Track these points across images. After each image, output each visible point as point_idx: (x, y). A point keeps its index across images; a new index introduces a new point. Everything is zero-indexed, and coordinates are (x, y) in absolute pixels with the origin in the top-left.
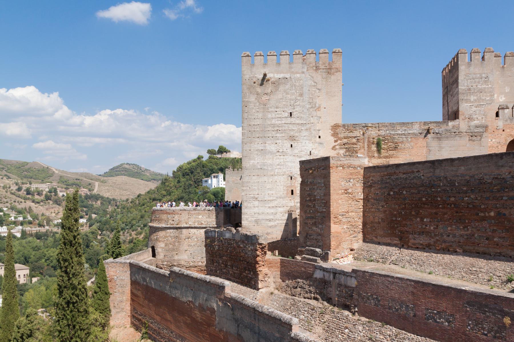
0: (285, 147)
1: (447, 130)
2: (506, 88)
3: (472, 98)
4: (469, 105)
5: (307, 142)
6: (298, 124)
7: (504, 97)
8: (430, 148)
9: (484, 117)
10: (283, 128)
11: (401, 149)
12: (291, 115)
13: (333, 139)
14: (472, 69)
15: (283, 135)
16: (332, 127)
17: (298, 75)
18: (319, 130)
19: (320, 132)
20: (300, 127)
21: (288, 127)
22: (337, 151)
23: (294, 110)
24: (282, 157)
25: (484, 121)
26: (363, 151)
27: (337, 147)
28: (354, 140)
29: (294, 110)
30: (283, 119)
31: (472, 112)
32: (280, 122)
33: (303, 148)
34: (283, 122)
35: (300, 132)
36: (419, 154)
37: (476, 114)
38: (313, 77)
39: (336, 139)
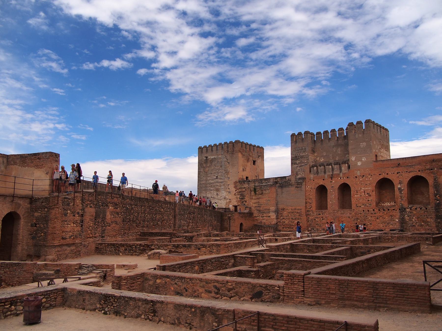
1: (285, 182)
2: (324, 153)
3: (298, 162)
6: (220, 182)
8: (277, 193)
11: (264, 194)
13: (234, 189)
14: (297, 144)
15: (214, 188)
17: (220, 156)
22: (236, 196)
26: (248, 195)
27: (236, 194)
34: (214, 181)
35: (221, 186)
36: (272, 197)
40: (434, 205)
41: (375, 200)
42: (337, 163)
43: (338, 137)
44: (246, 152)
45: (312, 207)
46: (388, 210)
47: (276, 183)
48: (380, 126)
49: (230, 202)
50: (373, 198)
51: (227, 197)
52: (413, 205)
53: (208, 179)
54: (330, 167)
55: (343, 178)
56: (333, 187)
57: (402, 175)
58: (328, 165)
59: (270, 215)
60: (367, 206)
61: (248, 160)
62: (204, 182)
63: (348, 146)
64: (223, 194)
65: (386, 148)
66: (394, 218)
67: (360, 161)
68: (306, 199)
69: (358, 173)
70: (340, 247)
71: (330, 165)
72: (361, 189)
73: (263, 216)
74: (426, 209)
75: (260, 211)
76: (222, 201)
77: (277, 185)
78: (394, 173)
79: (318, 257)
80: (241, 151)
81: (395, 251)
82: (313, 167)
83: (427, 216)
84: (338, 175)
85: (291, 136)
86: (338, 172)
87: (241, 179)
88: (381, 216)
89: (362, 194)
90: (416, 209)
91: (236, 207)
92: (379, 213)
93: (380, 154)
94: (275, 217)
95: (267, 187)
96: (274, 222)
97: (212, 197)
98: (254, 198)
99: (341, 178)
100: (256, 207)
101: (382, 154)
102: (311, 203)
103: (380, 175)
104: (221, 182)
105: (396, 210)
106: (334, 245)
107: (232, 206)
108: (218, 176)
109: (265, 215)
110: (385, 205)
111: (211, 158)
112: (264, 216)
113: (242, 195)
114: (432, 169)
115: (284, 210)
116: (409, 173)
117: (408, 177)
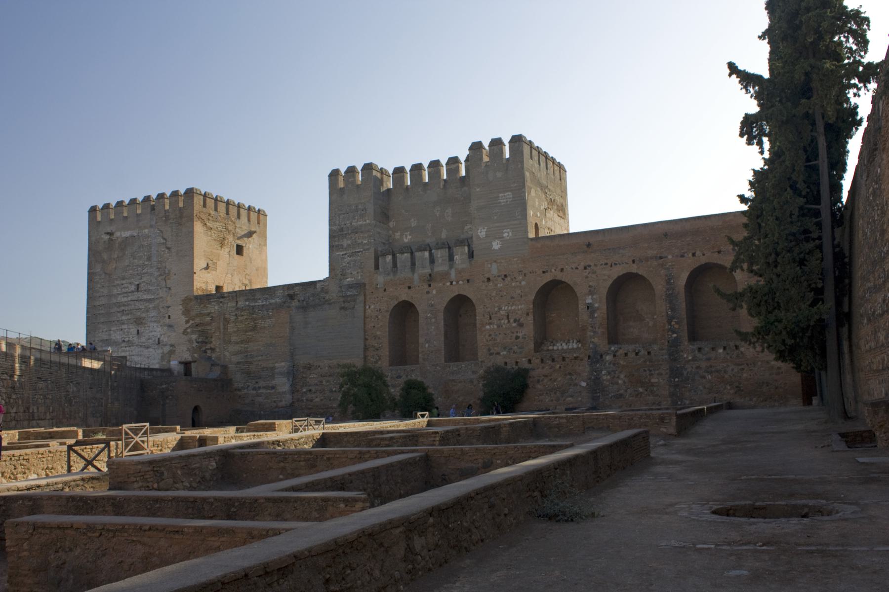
0: (131, 334)
1: (313, 295)
3: (346, 242)
4: (342, 253)
5: (155, 324)
7: (410, 235)
9: (360, 270)
10: (130, 308)
12: (138, 289)
13: (183, 319)
16: (183, 300)
17: (146, 231)
18: (168, 307)
19: (170, 309)
20: (147, 304)
21: (135, 305)
23: (141, 281)
24: (127, 348)
25: (360, 277)
27: (189, 330)
28: (208, 319)
29: (141, 281)
30: (130, 294)
31: (344, 264)
32: (126, 299)
33: (151, 334)
34: (129, 299)
35: (148, 311)
37: (350, 268)
38: (162, 232)
39: (187, 319)
40: (667, 343)
41: (532, 335)
42: (444, 244)
43: (445, 180)
44: (216, 220)
45: (380, 359)
46: (564, 359)
47: (291, 297)
48: (546, 155)
49: (171, 353)
50: (528, 331)
51: (164, 339)
52: (620, 346)
53: (115, 292)
54: (427, 254)
55: (457, 282)
56: (432, 305)
57: (594, 272)
58: (422, 249)
59: (274, 382)
60: (514, 352)
61: (222, 243)
62: (103, 301)
63: (470, 202)
64: (156, 330)
65: (559, 211)
66: (575, 379)
67: (497, 238)
68: (366, 339)
69: (494, 270)
70: (389, 454)
71: (425, 250)
72: (500, 309)
73: (257, 386)
74: (649, 353)
75: (248, 373)
76: (151, 350)
77: (295, 303)
78: (577, 268)
79: (252, 509)
80: (203, 217)
81: (576, 457)
82: (384, 255)
83: (650, 371)
84: (445, 276)
85: (331, 176)
86: (445, 268)
87: (203, 290)
88: (546, 376)
89: (503, 321)
90: (626, 354)
91: (187, 365)
92: (543, 368)
93: (546, 222)
94: (287, 388)
95: (267, 310)
96: (288, 399)
97: (124, 341)
98: (234, 339)
99: (451, 283)
100: (238, 363)
101: (549, 224)
102: (377, 350)
103: (544, 272)
104: (150, 300)
105: (582, 360)
106: (369, 452)
107: (176, 362)
108: (140, 283)
109: (261, 383)
110: (555, 348)
111: (124, 236)
112: (259, 388)
113: (203, 333)
114: (661, 258)
115: (309, 369)
116: (611, 266)
117: (609, 277)
